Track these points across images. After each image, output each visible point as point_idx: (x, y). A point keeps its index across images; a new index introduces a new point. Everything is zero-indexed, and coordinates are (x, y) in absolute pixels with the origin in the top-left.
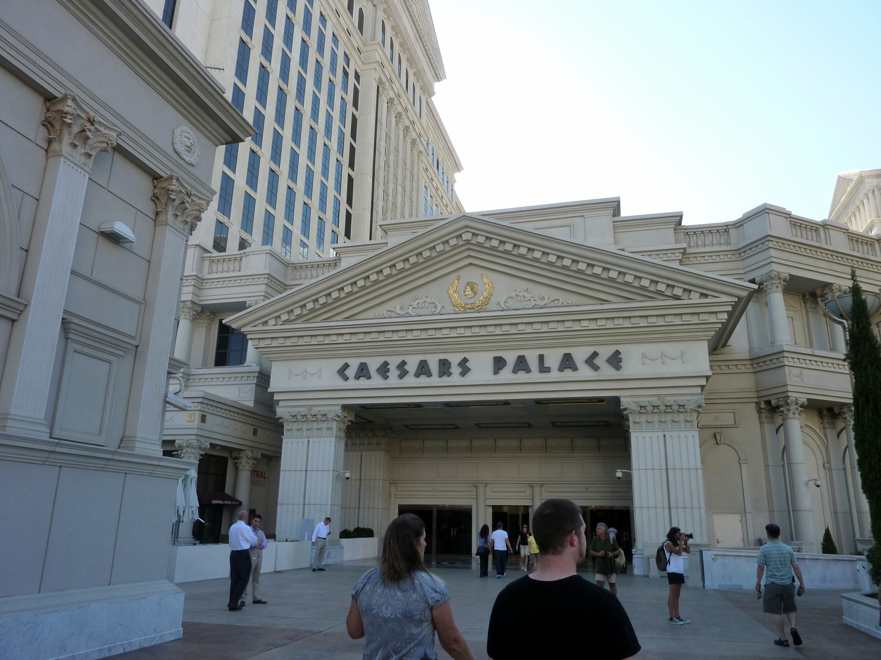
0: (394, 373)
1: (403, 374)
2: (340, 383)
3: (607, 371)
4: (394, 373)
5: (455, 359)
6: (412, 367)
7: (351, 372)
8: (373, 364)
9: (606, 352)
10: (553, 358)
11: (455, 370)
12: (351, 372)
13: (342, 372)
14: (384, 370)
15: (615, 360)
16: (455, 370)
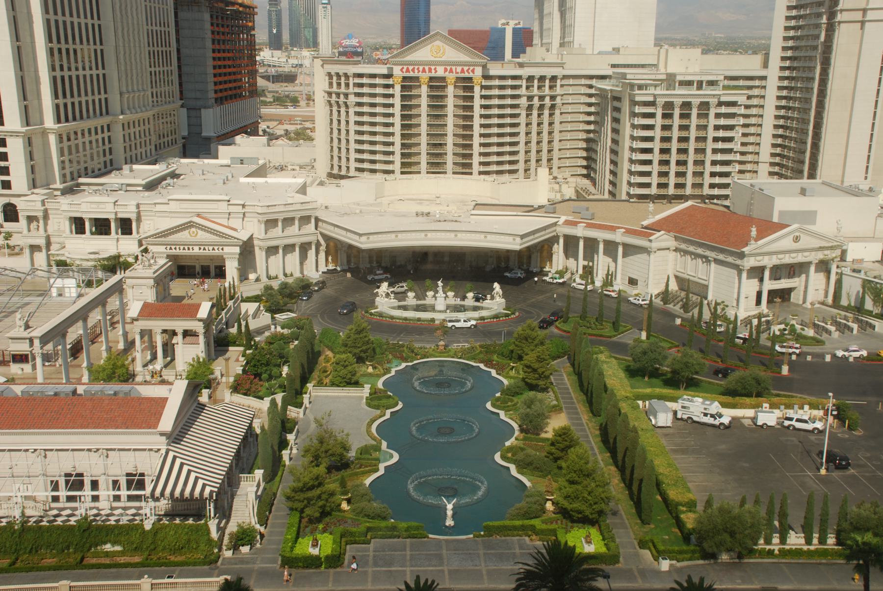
0: (416, 71)
1: (419, 72)
2: (401, 73)
4: (416, 71)
5: (433, 68)
6: (421, 69)
7: (404, 70)
8: (411, 68)
9: (471, 68)
10: (459, 69)
11: (433, 71)
12: (404, 70)
13: (402, 70)
14: (413, 70)
15: (473, 71)
16: (433, 71)
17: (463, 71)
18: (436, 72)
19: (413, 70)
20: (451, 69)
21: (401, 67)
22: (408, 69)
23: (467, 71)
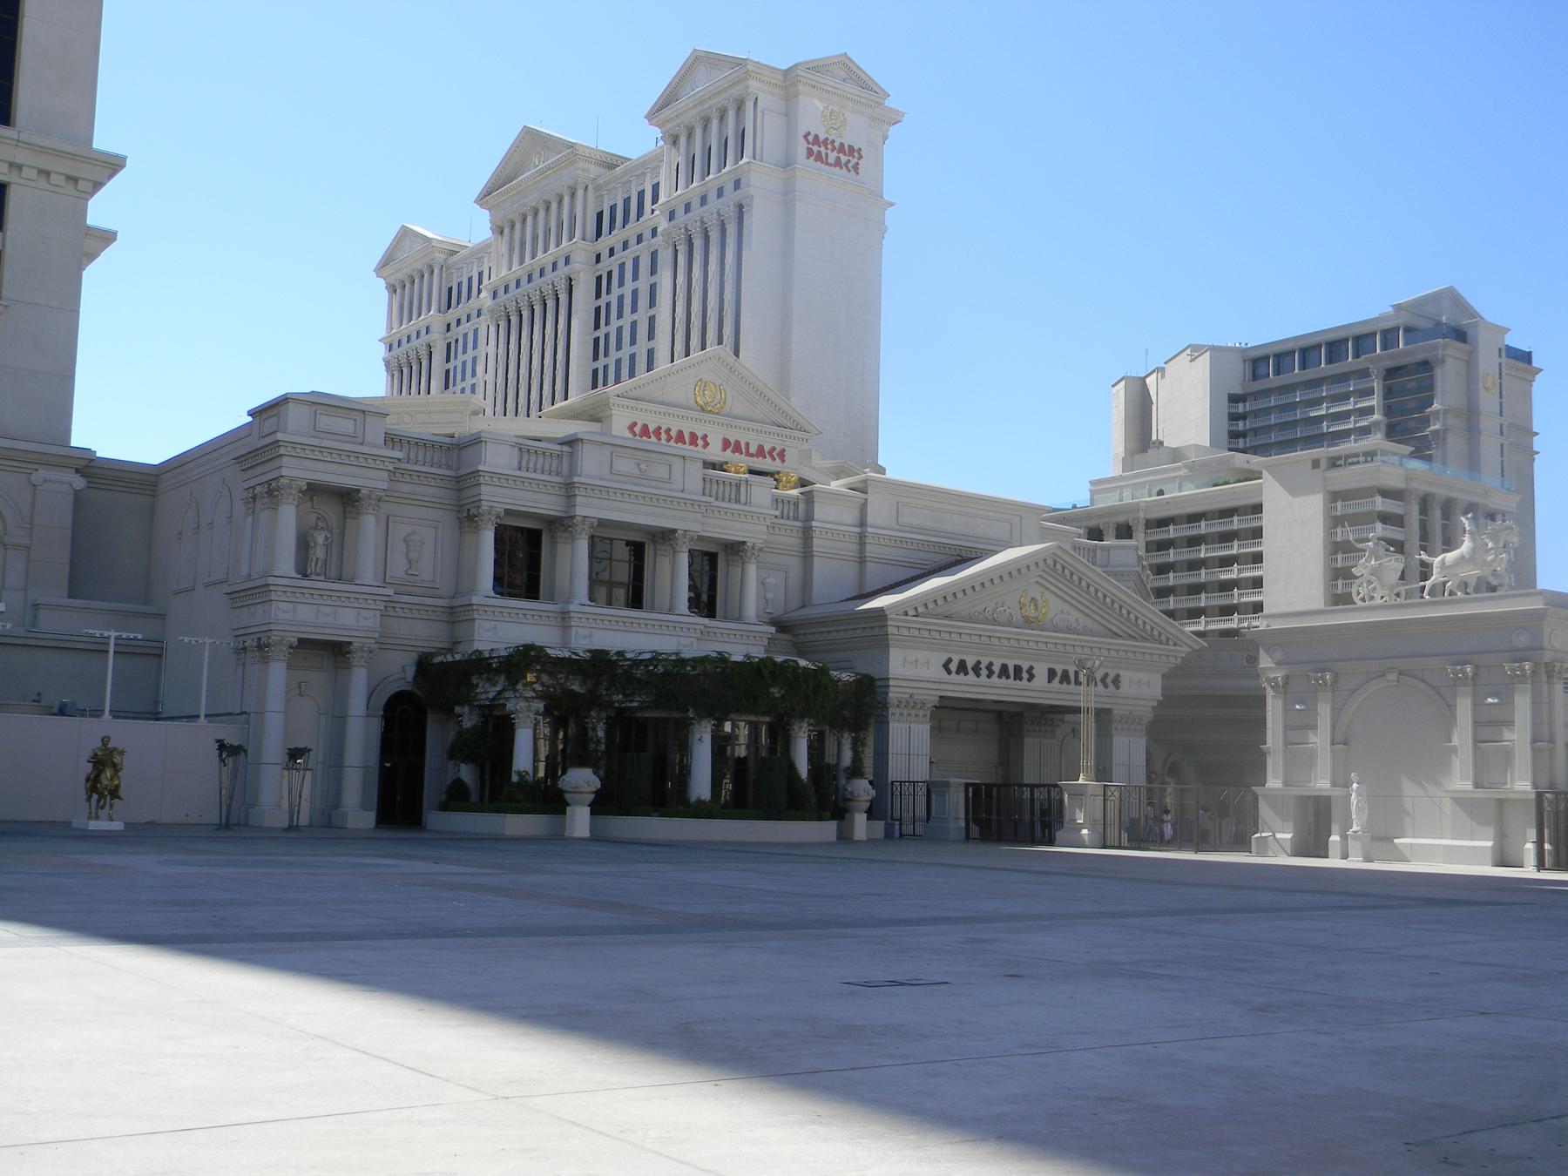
0: (664, 436)
1: (669, 439)
2: (628, 434)
3: (778, 461)
5: (700, 435)
9: (778, 449)
10: (753, 450)
11: (700, 442)
12: (637, 429)
13: (632, 427)
15: (782, 455)
17: (761, 452)
18: (706, 445)
19: (658, 431)
20: (738, 443)
21: (628, 422)
22: (645, 427)
23: (771, 453)
